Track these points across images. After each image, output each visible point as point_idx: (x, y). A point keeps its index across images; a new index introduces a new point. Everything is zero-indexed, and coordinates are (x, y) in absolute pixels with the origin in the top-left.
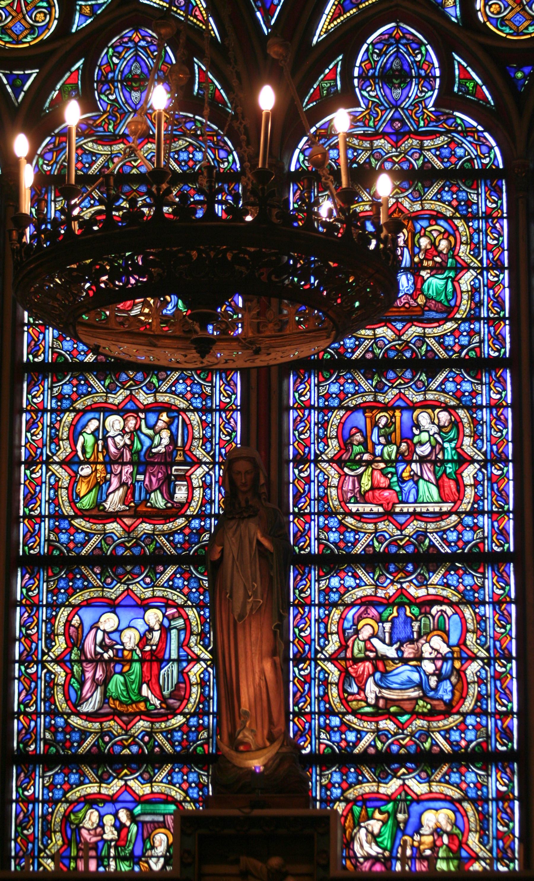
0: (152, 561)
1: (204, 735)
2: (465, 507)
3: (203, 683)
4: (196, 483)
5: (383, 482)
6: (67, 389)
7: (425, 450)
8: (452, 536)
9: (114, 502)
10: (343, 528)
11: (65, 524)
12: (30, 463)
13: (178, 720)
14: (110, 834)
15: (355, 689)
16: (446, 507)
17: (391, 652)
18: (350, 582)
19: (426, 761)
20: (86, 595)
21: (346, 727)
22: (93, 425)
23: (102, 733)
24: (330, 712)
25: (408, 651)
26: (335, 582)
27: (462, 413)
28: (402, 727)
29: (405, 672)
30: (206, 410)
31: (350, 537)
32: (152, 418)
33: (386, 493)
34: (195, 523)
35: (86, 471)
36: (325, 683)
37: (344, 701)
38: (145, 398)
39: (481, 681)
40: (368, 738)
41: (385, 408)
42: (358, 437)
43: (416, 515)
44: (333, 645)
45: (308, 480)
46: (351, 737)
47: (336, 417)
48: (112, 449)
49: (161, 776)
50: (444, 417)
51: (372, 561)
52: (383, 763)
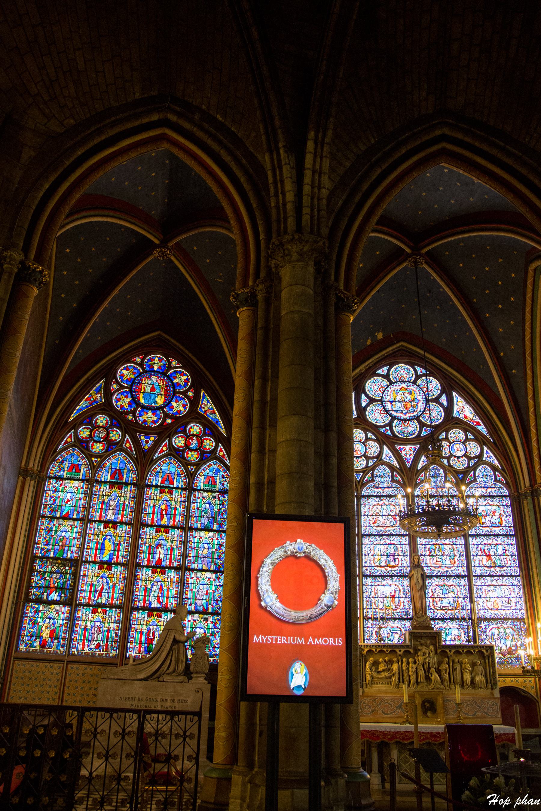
0: (392, 576)
1: (404, 613)
2: (456, 565)
3: (404, 602)
4: (400, 560)
5: (439, 560)
6: (372, 540)
7: (446, 554)
8: (454, 572)
9: (383, 564)
10: (431, 570)
11: (373, 568)
12: (365, 555)
13: (399, 610)
14: (386, 635)
15: (435, 604)
16: (452, 565)
17: (443, 596)
18: (433, 581)
19: (452, 619)
20: (378, 583)
21: (434, 612)
22: (378, 547)
23: (383, 613)
24: (431, 609)
25: (446, 596)
26: (430, 581)
27: (454, 546)
28: (446, 612)
29: (445, 601)
30: (401, 545)
31: (433, 572)
32: (390, 546)
33: (440, 563)
34: (400, 568)
35: (376, 557)
36: (429, 602)
37: (434, 606)
38: (388, 542)
39: (462, 603)
40: (439, 615)
41: (438, 545)
42: (433, 551)
43: (446, 567)
44: (430, 594)
45: (423, 559)
46: (436, 614)
47: (428, 546)
48: (382, 553)
49: (396, 622)
50: (450, 547)
51: (437, 577)
52: (442, 619)
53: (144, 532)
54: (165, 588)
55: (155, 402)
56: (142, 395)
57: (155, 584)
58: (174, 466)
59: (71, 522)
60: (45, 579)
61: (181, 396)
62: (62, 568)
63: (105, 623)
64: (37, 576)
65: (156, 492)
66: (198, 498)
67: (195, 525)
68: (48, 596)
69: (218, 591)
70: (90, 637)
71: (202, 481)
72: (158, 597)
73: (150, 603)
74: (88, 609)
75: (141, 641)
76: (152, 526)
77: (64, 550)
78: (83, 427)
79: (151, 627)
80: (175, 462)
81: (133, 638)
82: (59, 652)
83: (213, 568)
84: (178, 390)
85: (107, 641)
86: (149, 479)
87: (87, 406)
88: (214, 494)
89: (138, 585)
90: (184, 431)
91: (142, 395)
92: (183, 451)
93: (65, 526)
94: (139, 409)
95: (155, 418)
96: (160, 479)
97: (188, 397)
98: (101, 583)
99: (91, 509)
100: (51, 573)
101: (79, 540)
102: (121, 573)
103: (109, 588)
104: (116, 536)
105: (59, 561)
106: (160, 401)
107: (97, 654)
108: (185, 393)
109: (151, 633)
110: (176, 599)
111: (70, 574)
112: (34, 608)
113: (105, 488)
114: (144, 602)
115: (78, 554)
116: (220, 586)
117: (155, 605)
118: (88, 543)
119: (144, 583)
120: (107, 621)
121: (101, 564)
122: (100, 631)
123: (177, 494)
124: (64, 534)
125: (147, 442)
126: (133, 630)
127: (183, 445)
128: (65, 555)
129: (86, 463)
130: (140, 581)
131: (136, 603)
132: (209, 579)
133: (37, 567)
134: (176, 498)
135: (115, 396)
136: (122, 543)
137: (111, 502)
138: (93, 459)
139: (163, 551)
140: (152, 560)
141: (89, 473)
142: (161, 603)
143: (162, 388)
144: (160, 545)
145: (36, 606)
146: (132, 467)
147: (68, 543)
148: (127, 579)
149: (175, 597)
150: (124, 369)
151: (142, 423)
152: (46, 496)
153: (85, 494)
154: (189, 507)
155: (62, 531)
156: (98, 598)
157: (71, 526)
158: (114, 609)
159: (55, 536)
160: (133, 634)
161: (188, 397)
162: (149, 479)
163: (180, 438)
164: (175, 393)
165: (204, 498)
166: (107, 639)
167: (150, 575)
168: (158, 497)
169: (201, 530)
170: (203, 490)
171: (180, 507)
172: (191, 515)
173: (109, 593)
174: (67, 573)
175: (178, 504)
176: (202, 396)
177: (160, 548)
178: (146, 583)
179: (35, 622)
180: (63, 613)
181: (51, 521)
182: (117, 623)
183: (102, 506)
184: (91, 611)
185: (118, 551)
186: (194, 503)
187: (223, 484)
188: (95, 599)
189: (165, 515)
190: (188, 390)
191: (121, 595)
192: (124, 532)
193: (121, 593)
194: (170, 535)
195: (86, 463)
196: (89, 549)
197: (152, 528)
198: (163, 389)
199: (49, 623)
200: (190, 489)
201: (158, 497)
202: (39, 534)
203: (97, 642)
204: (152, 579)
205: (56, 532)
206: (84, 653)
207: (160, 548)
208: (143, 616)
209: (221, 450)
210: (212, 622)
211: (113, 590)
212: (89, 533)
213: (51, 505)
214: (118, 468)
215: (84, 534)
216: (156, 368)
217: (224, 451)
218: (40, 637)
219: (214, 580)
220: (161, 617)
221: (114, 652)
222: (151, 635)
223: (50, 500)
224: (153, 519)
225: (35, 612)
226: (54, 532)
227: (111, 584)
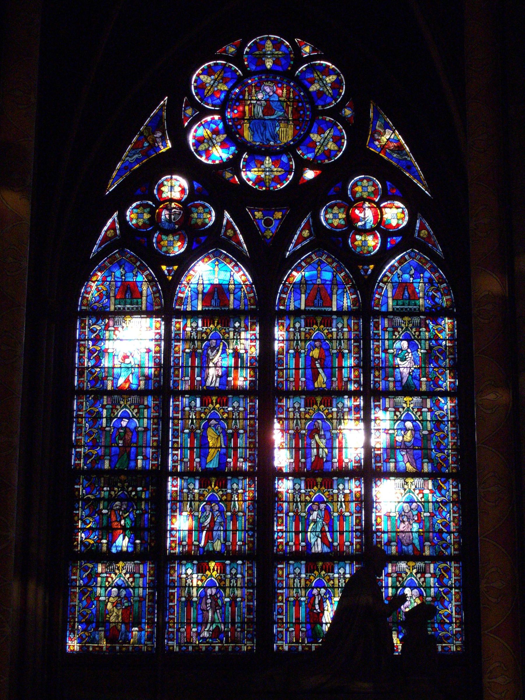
53: (282, 406)
54: (336, 514)
55: (275, 137)
56: (246, 126)
57: (315, 507)
58: (328, 267)
59: (134, 398)
60: (100, 513)
61: (328, 119)
62: (130, 489)
63: (224, 589)
64: (83, 509)
65: (297, 325)
66: (384, 329)
67: (382, 386)
68: (110, 544)
69: (440, 513)
70: (200, 617)
71: (390, 294)
72: (323, 531)
73: (309, 545)
74: (189, 565)
75: (297, 619)
76: (296, 393)
78: (134, 205)
79: (315, 591)
80: (330, 260)
81: (281, 614)
82: (145, 649)
83: (427, 468)
84: (320, 108)
85: (233, 623)
86: (281, 299)
87: (137, 161)
88: (416, 320)
89: (281, 512)
90: (342, 194)
91: (246, 126)
92: (345, 235)
93: (125, 407)
94: (245, 156)
95: (278, 171)
96: (303, 296)
97: (343, 120)
98: (208, 512)
99: (172, 370)
100: (110, 500)
102: (245, 491)
103: (225, 522)
104: (227, 418)
105: (123, 477)
106: (286, 134)
107: (217, 649)
108: (336, 112)
109: (317, 602)
110: (358, 534)
111: (145, 500)
112: (86, 569)
113: (194, 325)
114: (297, 544)
115: (156, 459)
116: (445, 503)
117: (318, 547)
118: (174, 437)
119: (292, 506)
120: (228, 584)
121: (205, 476)
122: (217, 605)
123: (340, 326)
124: (124, 423)
125: (268, 223)
126: (280, 598)
127: (343, 222)
128: (132, 464)
129: (150, 278)
130: (285, 505)
131: (280, 547)
132: (421, 491)
133: (82, 492)
134: (340, 334)
135: (192, 133)
136: (241, 431)
137: (209, 352)
138: (164, 268)
139: (324, 441)
140: (303, 460)
141: (159, 297)
142: (330, 545)
143: (288, 106)
144: (317, 431)
145: (90, 566)
146: (244, 278)
148: (257, 502)
149: (357, 531)
150: (204, 72)
151: (255, 183)
152: (80, 352)
153: (156, 340)
154: (367, 349)
155: (121, 418)
156: (206, 542)
157: (137, 406)
158: (240, 562)
159: (107, 429)
160: (281, 607)
161: (343, 120)
162: (281, 299)
163: (336, 208)
164: (316, 113)
165: (395, 329)
166: (233, 619)
167: (303, 491)
168: (303, 334)
169: (396, 394)
170: (395, 313)
171: (350, 352)
172: (372, 364)
173: (225, 531)
174: (140, 499)
175: (344, 345)
176: (371, 115)
177: (317, 437)
178: (297, 507)
179: (93, 596)
180: (143, 576)
181: (96, 399)
182: (248, 588)
183: (193, 362)
184: (195, 568)
185: (235, 448)
186: (378, 341)
187: (433, 298)
188: (202, 544)
189: (320, 371)
190: (341, 106)
191: (251, 533)
192: (241, 409)
193: (250, 529)
194: (335, 409)
195: (150, 278)
196: (177, 449)
197: (297, 399)
198: (290, 108)
199: (118, 595)
200: (365, 311)
201: (303, 334)
203: (214, 626)
204: (307, 498)
206: (190, 648)
207: (317, 437)
208: (297, 571)
209: (422, 227)
210: (434, 575)
211: (234, 525)
212: (174, 418)
213: (93, 367)
214: (216, 282)
215: (163, 419)
216: (269, 64)
217: (428, 227)
218: (106, 623)
219: (432, 492)
220: (333, 572)
221: (249, 644)
222: (317, 607)
223: (89, 358)
224: (297, 380)
225: (89, 577)
226: (104, 420)
227: (229, 514)
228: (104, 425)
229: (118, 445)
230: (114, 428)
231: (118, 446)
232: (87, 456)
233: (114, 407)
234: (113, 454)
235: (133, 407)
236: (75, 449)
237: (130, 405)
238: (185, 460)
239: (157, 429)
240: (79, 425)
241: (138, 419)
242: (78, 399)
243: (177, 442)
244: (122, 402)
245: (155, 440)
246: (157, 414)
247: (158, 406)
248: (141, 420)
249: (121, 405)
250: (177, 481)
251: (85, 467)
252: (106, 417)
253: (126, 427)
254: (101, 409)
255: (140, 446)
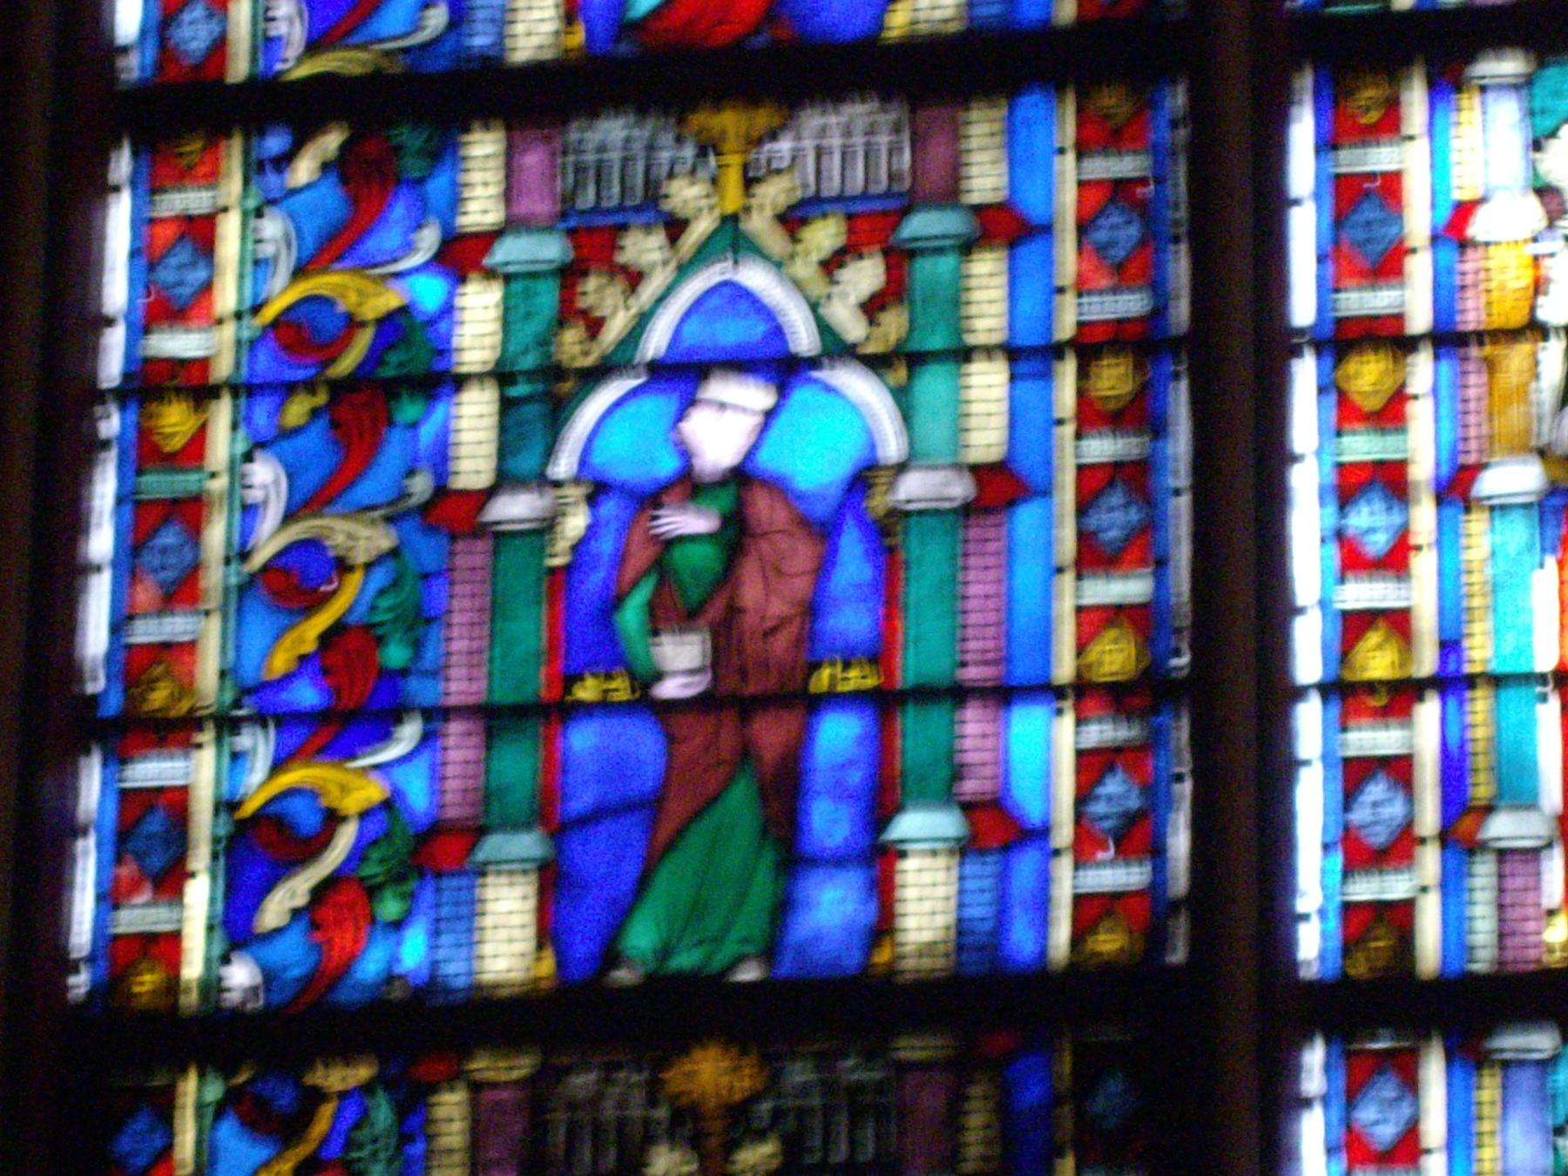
59: (841, 141)
77: (785, 792)
93: (732, 237)
101: (1115, 518)
105: (711, 1073)
115: (1137, 835)
128: (832, 905)
147: (851, 620)
155: (682, 375)
157: (874, 224)
159: (515, 508)
181: (368, 179)
202: (144, 519)
205: (539, 394)
212: (1343, 340)
226: (473, 419)
228: (474, 465)
229: (646, 680)
230: (598, 489)
231: (645, 703)
232: (262, 845)
233: (594, 246)
234: (582, 800)
235: (825, 235)
236: (118, 757)
237: (793, 220)
238: (1503, 827)
239: (1134, 477)
240: (159, 484)
241: (898, 363)
242: (150, 185)
243: (1398, 622)
244: (685, 194)
245: (1114, 614)
246: (1132, 304)
247: (1146, 212)
248: (932, 383)
249: (675, 227)
250: (1411, 1084)
251: (241, 975)
252: (502, 375)
253: (742, 476)
254: (429, 292)
255: (925, 694)
